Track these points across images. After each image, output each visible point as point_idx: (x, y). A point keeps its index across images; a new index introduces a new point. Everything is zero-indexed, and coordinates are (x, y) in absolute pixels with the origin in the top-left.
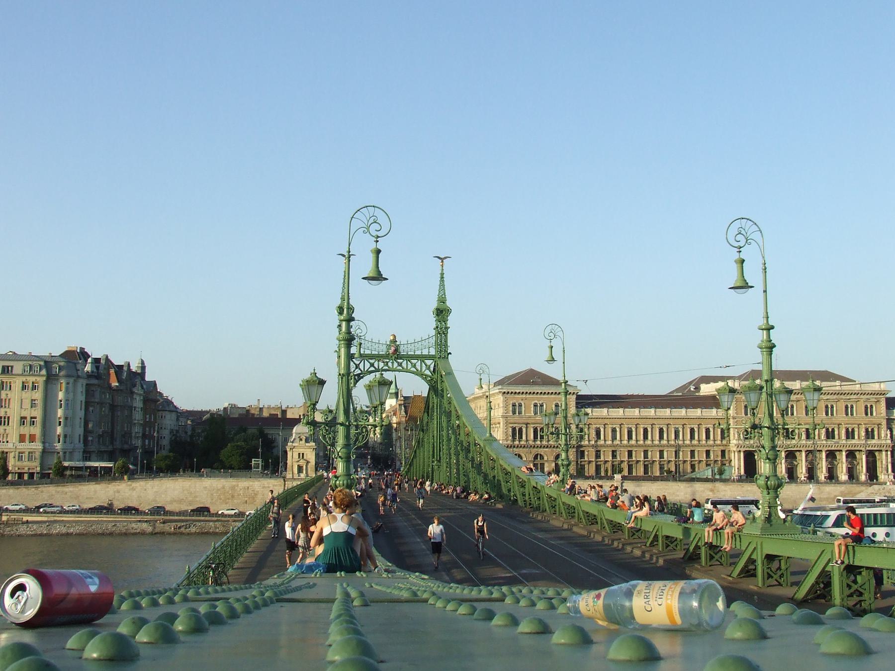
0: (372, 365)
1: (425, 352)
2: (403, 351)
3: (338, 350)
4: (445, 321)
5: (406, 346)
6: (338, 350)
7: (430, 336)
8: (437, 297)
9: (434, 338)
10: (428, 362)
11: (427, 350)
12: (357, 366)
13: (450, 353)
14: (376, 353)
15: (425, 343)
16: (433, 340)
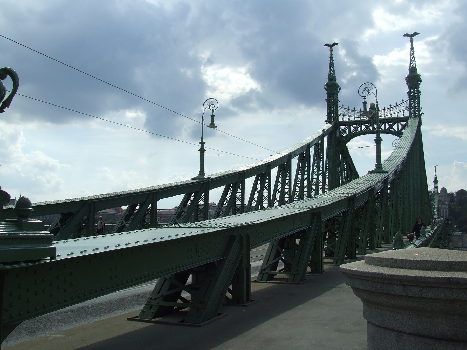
0: (356, 129)
1: (400, 115)
2: (382, 114)
3: (327, 120)
4: (417, 86)
5: (383, 112)
6: (327, 120)
7: (404, 101)
8: (409, 68)
9: (408, 103)
10: (403, 123)
11: (402, 113)
12: (344, 131)
13: (423, 113)
14: (359, 119)
15: (400, 108)
16: (407, 105)
